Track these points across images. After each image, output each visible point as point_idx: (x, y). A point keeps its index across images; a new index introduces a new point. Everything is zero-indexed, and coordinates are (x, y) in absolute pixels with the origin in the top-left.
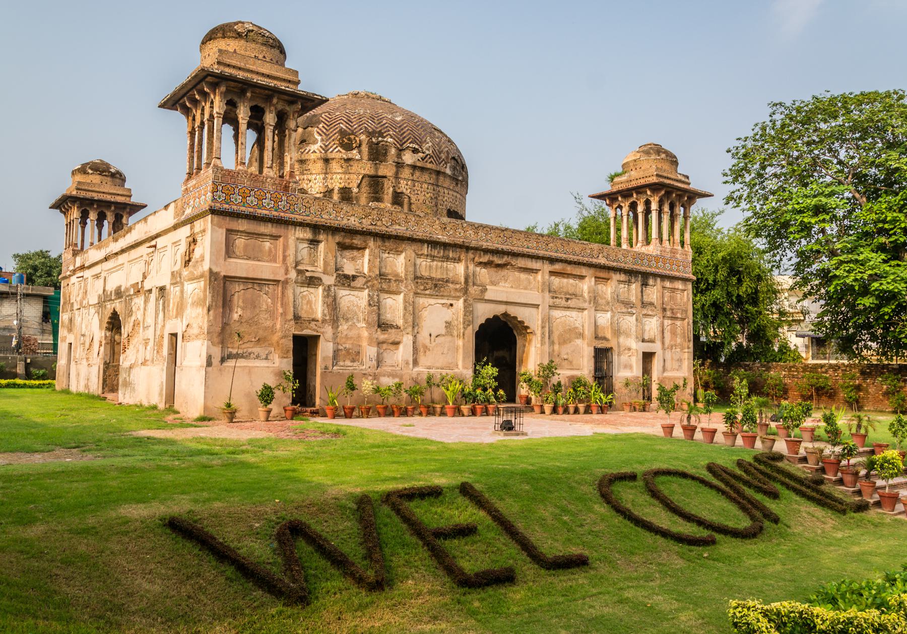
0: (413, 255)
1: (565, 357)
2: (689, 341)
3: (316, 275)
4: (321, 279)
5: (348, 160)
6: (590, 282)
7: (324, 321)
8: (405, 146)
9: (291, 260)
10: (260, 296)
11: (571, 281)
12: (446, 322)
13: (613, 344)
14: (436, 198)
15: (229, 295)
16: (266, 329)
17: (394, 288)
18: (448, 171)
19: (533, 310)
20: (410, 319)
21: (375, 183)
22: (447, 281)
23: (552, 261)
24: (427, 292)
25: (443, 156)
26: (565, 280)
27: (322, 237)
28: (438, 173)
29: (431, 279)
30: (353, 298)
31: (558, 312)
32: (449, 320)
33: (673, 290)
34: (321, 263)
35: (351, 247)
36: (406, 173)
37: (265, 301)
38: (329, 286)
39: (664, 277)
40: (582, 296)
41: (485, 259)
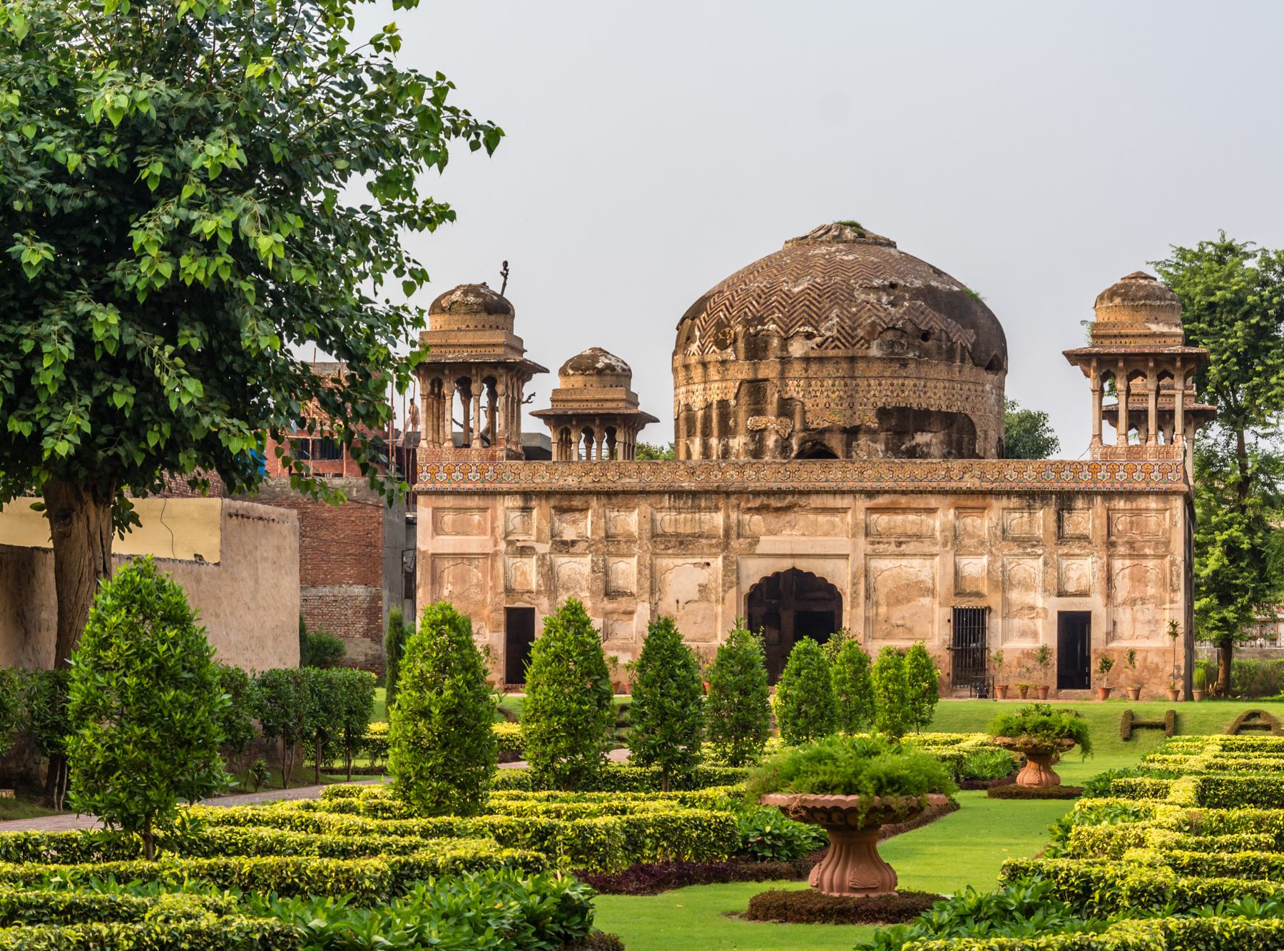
0: (650, 509)
1: (899, 622)
2: (1174, 591)
3: (527, 544)
4: (533, 548)
5: (723, 362)
6: (946, 516)
7: (539, 592)
8: (792, 332)
9: (500, 531)
10: (470, 571)
11: (912, 517)
12: (700, 585)
13: (994, 600)
14: (852, 396)
15: (438, 571)
16: (476, 603)
17: (625, 551)
18: (875, 351)
19: (842, 563)
20: (647, 584)
21: (755, 389)
22: (700, 536)
23: (871, 494)
24: (670, 551)
25: (860, 332)
26: (899, 518)
27: (534, 503)
28: (852, 360)
29: (677, 535)
30: (573, 565)
31: (887, 562)
32: (703, 581)
33: (1138, 512)
34: (534, 531)
35: (571, 510)
36: (796, 369)
37: (476, 575)
38: (544, 555)
39: (1108, 495)
40: (932, 537)
41: (756, 503)
